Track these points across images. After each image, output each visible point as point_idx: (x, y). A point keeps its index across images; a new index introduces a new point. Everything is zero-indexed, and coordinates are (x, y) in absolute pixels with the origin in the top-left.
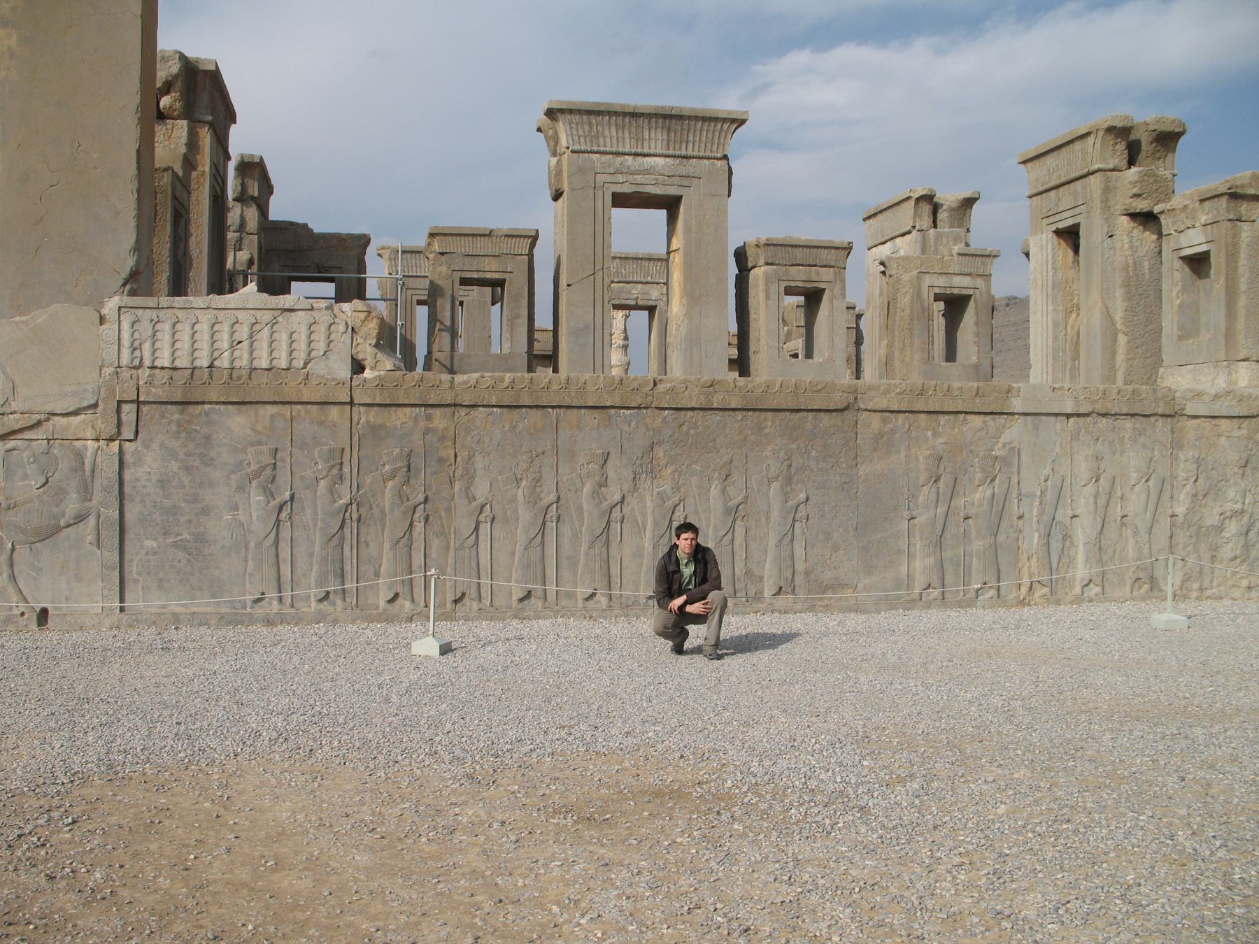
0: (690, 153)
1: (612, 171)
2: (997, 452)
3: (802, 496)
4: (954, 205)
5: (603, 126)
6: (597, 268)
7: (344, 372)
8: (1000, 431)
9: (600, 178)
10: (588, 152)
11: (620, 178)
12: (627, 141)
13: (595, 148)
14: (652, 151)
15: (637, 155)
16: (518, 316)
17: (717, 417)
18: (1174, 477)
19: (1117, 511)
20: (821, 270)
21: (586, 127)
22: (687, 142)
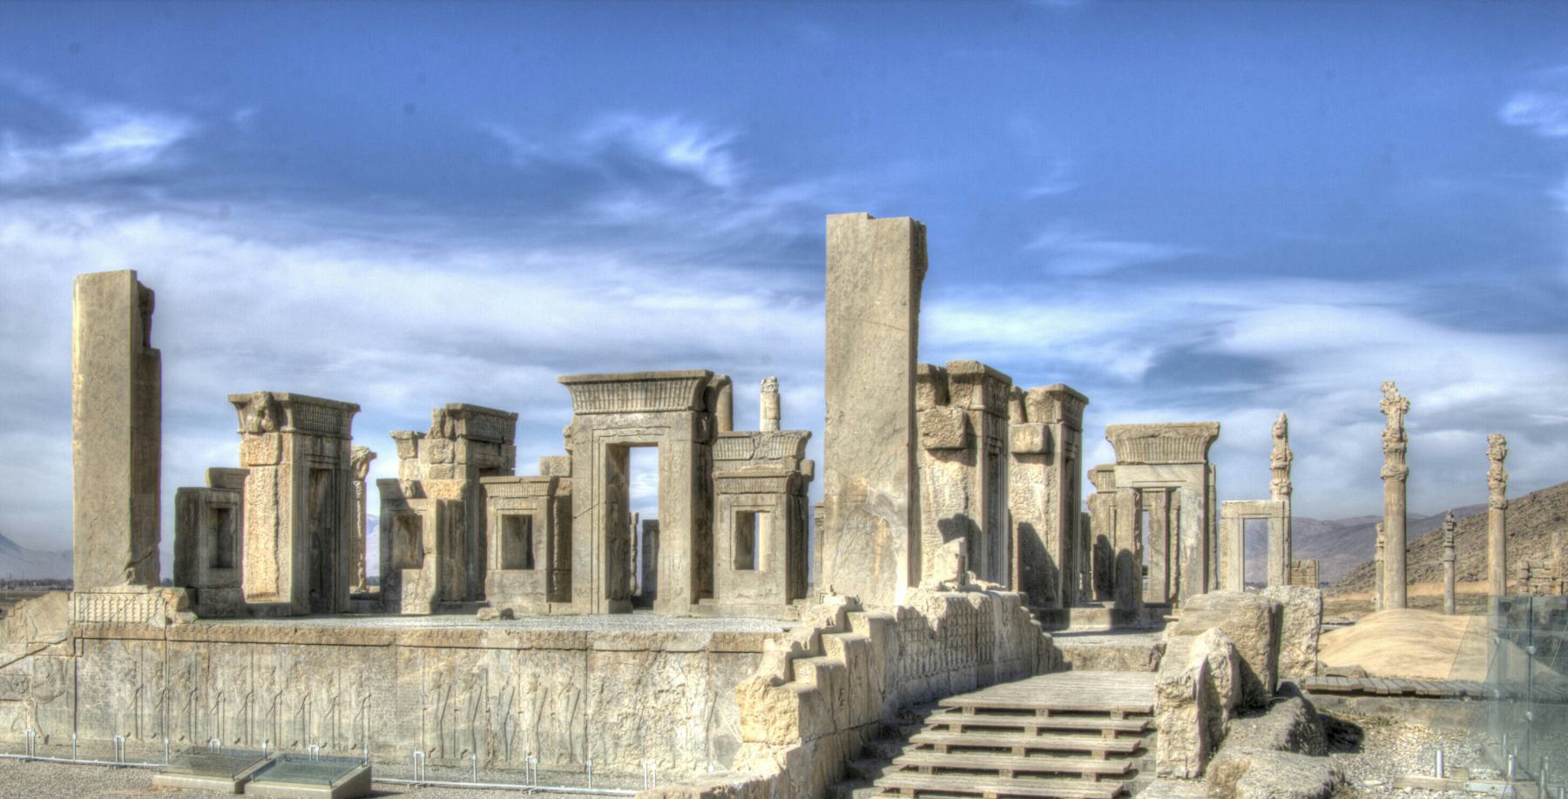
0: (662, 408)
1: (605, 427)
2: (475, 670)
3: (367, 694)
4: (1039, 398)
5: (598, 391)
6: (595, 502)
7: (162, 625)
8: (478, 657)
9: (597, 433)
10: (590, 414)
11: (611, 432)
12: (616, 402)
13: (592, 411)
14: (633, 409)
15: (622, 413)
16: (540, 542)
17: (325, 649)
18: (586, 689)
19: (547, 711)
20: (765, 496)
21: (587, 394)
22: (660, 399)
